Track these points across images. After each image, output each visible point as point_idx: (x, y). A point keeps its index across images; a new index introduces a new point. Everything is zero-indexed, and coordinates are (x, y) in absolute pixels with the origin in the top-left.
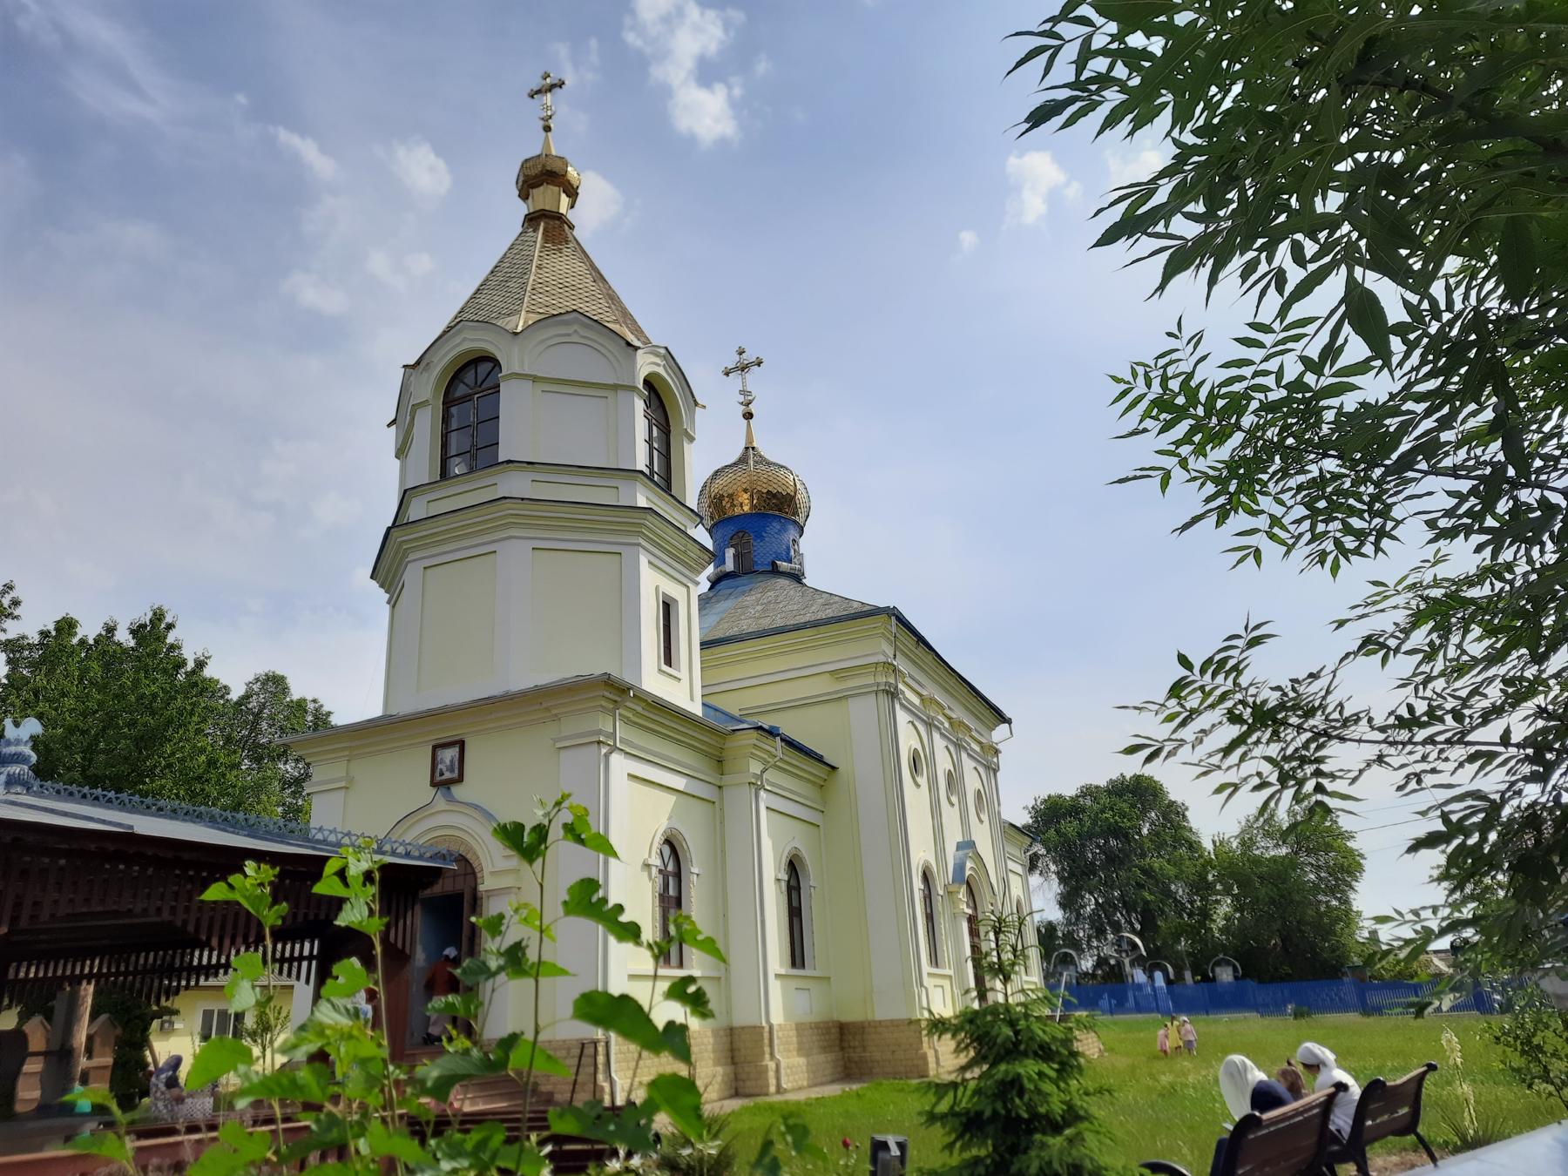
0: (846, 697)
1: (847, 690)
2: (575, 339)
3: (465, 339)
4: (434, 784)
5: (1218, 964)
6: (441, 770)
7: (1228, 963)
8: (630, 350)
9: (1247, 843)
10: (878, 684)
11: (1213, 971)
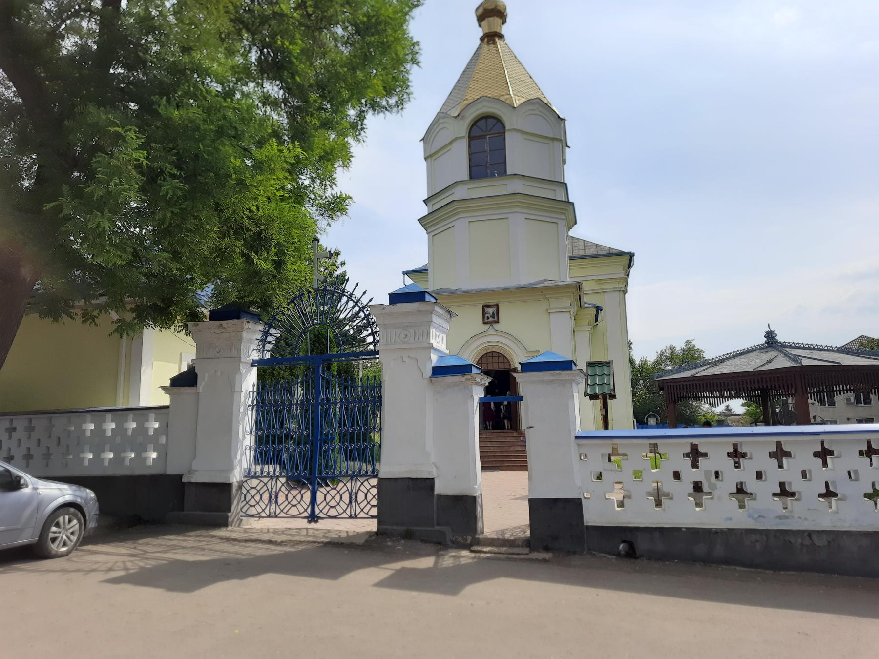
0: (603, 292)
1: (606, 289)
2: (537, 112)
4: (484, 323)
5: (649, 416)
7: (655, 417)
8: (559, 120)
9: (658, 362)
10: (621, 288)
11: (647, 419)
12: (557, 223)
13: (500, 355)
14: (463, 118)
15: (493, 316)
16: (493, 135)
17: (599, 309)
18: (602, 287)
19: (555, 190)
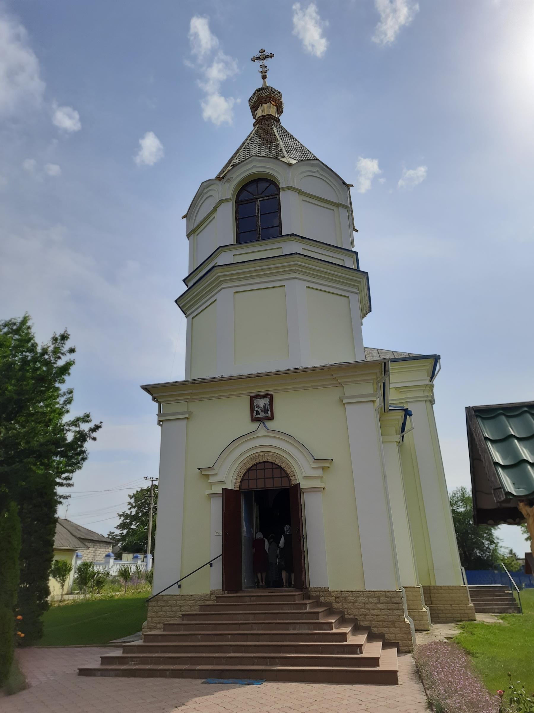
1: (408, 398)
2: (317, 175)
3: (254, 166)
4: (253, 420)
6: (257, 412)
10: (427, 396)
12: (348, 297)
13: (274, 466)
14: (229, 180)
15: (265, 411)
16: (265, 198)
17: (407, 413)
18: (404, 396)
19: (343, 260)
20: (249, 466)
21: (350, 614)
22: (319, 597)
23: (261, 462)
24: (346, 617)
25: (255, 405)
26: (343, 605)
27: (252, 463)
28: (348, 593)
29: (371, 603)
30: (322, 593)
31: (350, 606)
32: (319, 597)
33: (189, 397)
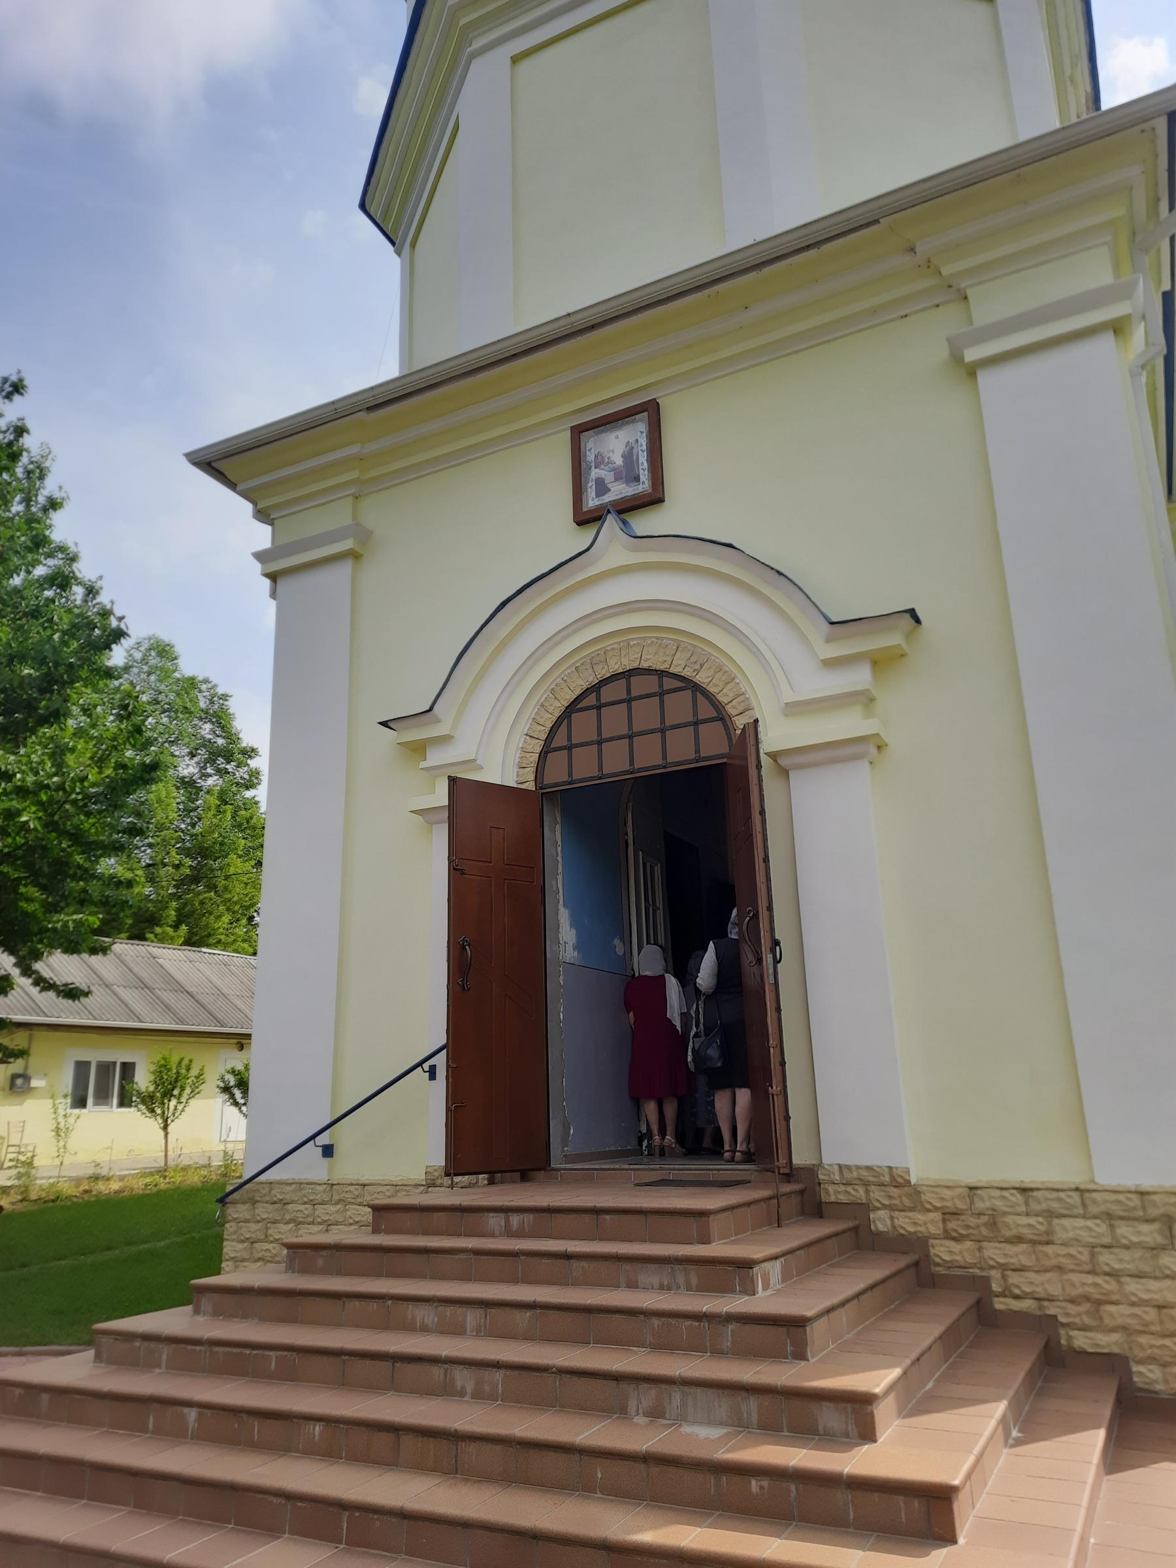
4: (586, 519)
13: (669, 683)
15: (628, 474)
20: (569, 696)
21: (1017, 1291)
22: (864, 1208)
23: (614, 677)
24: (999, 1304)
25: (591, 457)
26: (980, 1249)
27: (581, 683)
28: (1003, 1197)
29: (1127, 1247)
30: (877, 1194)
31: (1018, 1254)
32: (864, 1208)
33: (354, 475)
